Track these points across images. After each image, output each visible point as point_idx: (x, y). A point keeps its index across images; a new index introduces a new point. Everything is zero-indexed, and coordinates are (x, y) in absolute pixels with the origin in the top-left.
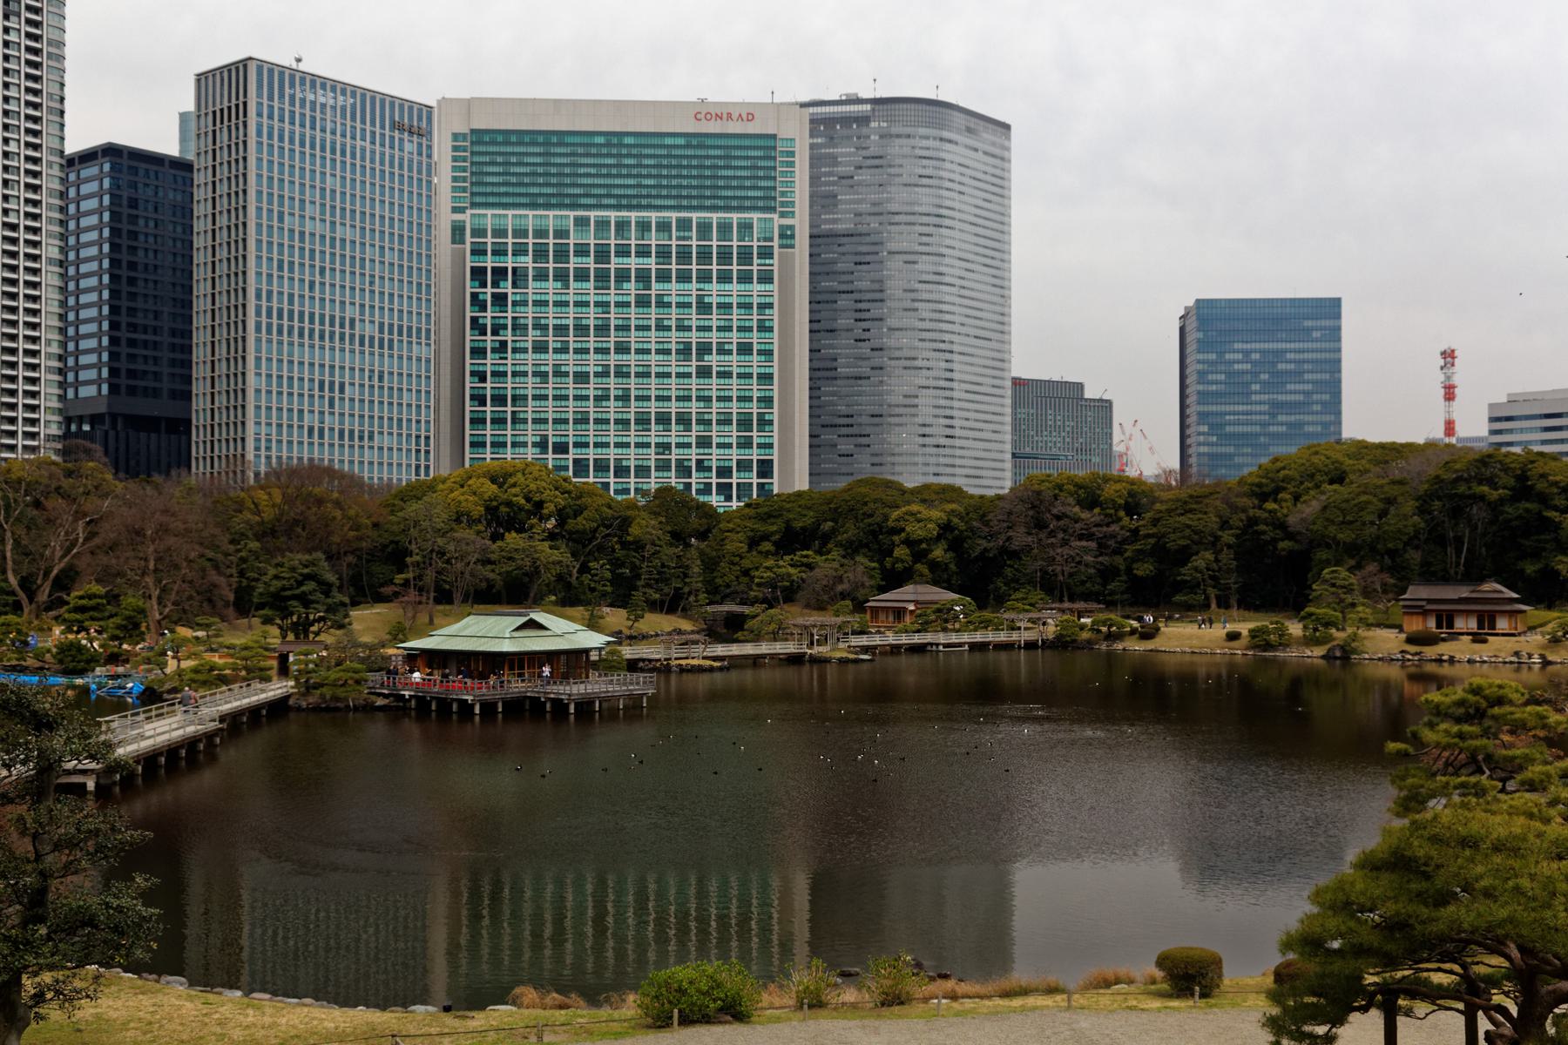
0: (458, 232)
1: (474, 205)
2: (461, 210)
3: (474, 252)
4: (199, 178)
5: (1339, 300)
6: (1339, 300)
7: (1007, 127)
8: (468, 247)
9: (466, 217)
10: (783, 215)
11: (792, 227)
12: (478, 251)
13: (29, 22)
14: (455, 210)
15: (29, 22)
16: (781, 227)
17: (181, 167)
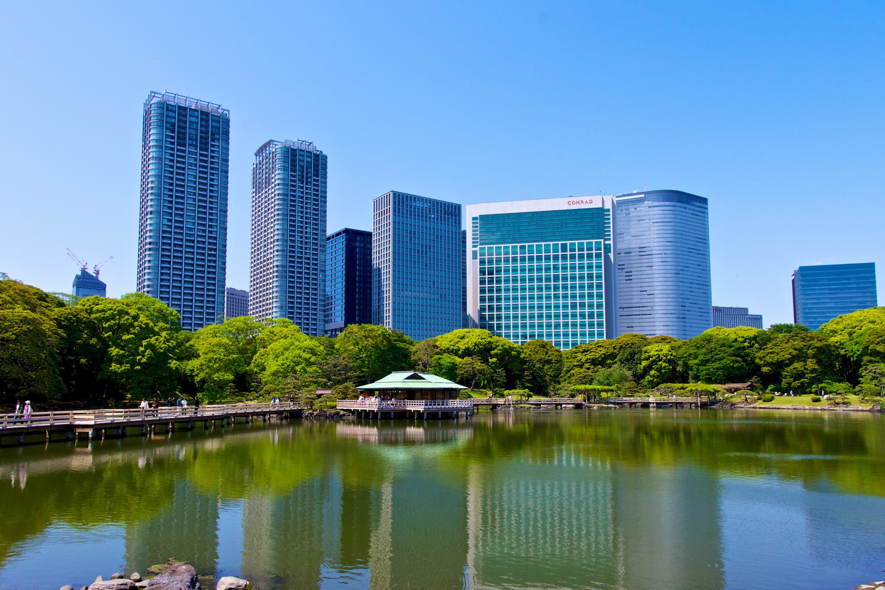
0: (474, 254)
1: (481, 244)
2: (476, 246)
3: (481, 262)
4: (374, 238)
5: (873, 264)
6: (873, 264)
7: (704, 201)
8: (478, 260)
9: (477, 249)
10: (605, 240)
11: (610, 245)
12: (482, 262)
13: (314, 185)
14: (474, 246)
15: (314, 185)
16: (605, 244)
17: (369, 235)
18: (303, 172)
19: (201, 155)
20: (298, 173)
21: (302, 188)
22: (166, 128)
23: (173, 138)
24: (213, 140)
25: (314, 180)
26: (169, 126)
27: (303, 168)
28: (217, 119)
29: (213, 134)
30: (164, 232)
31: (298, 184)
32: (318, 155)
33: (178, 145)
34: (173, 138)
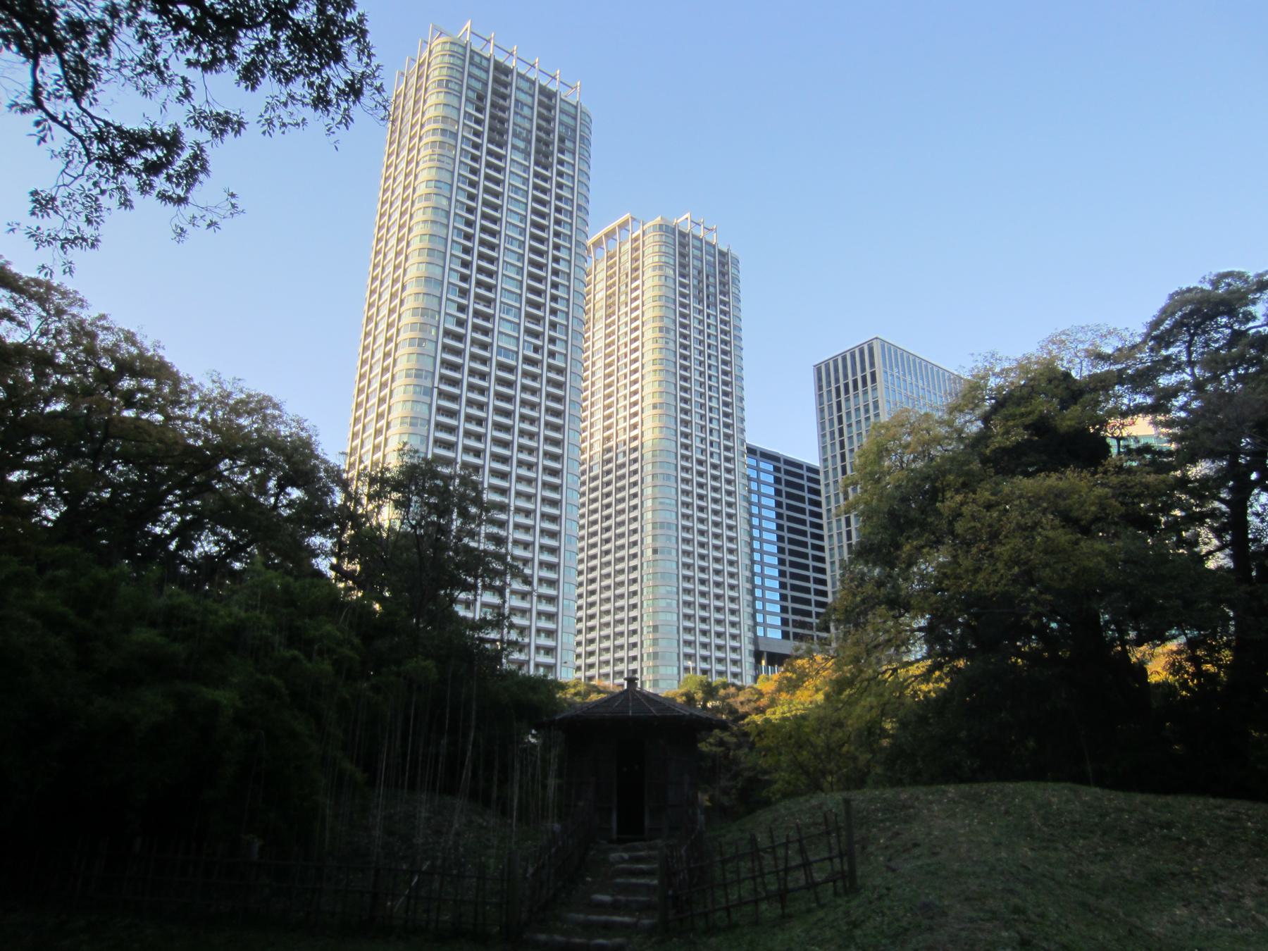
18: (700, 281)
19: (537, 175)
20: (692, 282)
21: (701, 312)
22: (467, 100)
23: (479, 122)
24: (561, 151)
25: (722, 302)
26: (473, 95)
27: (700, 272)
28: (572, 111)
29: (562, 140)
30: (447, 333)
31: (693, 303)
32: (722, 254)
33: (490, 141)
34: (479, 122)
